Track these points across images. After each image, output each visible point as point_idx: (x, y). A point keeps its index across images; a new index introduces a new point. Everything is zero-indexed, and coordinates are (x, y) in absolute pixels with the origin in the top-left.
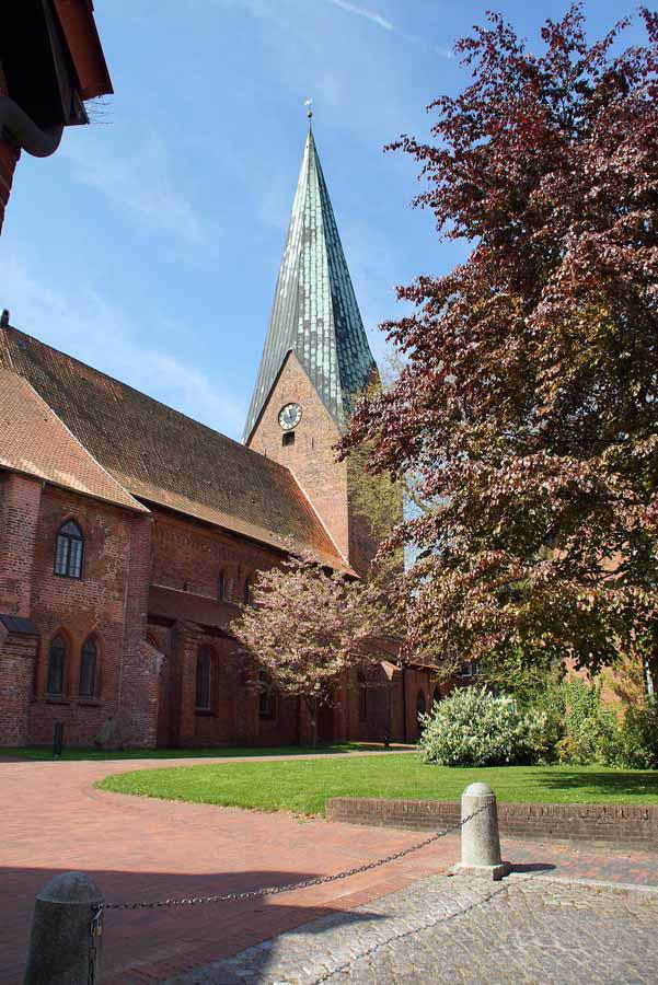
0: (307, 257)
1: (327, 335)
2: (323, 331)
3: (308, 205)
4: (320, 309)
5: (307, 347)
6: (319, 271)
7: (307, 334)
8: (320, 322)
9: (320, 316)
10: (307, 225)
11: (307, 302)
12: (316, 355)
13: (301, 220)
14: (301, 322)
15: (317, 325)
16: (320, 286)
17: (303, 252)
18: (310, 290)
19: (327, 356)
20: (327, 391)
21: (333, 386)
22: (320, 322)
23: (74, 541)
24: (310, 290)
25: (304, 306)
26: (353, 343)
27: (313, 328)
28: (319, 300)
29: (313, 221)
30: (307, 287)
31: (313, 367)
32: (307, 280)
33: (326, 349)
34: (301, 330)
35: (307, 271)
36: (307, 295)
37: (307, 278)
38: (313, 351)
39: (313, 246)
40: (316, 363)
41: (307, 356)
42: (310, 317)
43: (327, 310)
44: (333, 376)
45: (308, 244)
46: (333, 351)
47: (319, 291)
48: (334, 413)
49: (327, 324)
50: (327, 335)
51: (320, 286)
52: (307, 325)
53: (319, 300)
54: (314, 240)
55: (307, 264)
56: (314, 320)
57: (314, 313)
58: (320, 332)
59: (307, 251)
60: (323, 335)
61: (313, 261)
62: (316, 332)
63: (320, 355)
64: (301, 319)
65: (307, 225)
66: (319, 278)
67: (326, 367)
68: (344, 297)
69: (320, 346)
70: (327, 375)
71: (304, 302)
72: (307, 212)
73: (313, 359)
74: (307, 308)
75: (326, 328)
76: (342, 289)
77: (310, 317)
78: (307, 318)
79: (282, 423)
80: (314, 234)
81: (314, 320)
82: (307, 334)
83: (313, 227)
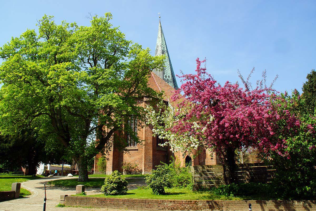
1: (171, 80)
4: (168, 73)
7: (166, 79)
13: (161, 47)
14: (164, 76)
27: (167, 78)
36: (165, 69)
47: (168, 68)
49: (171, 78)
50: (171, 80)
51: (168, 67)
52: (166, 77)
54: (165, 54)
57: (167, 74)
58: (169, 79)
60: (170, 80)
64: (164, 75)
69: (170, 83)
74: (165, 72)
75: (171, 78)
80: (165, 52)
81: (167, 76)
83: (164, 50)
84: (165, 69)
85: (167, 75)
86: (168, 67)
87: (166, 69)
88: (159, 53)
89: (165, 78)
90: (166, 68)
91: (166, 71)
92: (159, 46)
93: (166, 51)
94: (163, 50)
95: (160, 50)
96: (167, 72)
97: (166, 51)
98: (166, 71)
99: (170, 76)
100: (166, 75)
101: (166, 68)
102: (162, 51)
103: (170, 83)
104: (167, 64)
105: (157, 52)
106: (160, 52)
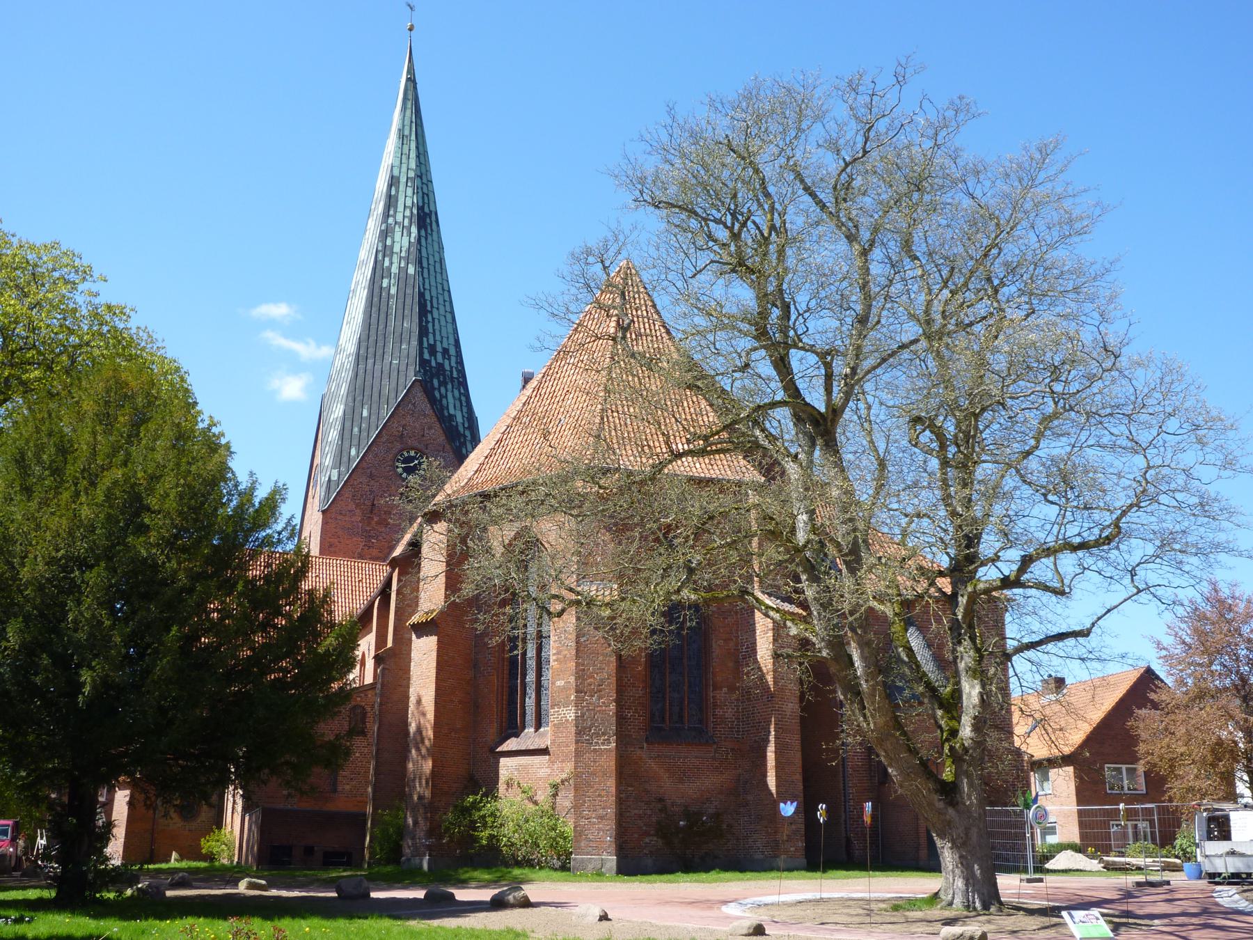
2: (451, 367)
4: (444, 334)
5: (436, 382)
7: (433, 364)
9: (445, 345)
12: (446, 397)
14: (425, 345)
15: (444, 358)
27: (439, 357)
28: (443, 323)
33: (456, 392)
36: (429, 308)
37: (427, 281)
39: (429, 237)
51: (441, 301)
53: (442, 319)
54: (429, 231)
58: (447, 367)
60: (451, 372)
61: (431, 262)
64: (425, 339)
69: (449, 386)
70: (461, 429)
71: (426, 318)
73: (444, 402)
74: (430, 325)
77: (435, 341)
80: (428, 221)
81: (439, 348)
84: (431, 312)
85: (438, 344)
86: (441, 301)
88: (399, 217)
89: (426, 356)
90: (432, 307)
92: (403, 180)
94: (423, 207)
96: (437, 327)
98: (433, 319)
100: (432, 342)
101: (432, 307)
102: (415, 211)
103: (449, 386)
104: (440, 287)
105: (391, 212)
106: (408, 213)
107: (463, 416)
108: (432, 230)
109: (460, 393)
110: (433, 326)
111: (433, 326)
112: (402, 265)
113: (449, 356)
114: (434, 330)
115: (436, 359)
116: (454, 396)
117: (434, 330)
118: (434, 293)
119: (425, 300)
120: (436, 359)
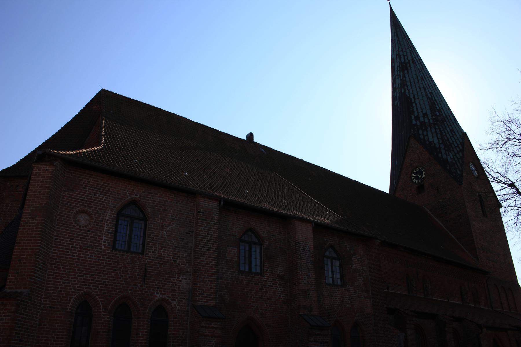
0: (408, 79)
1: (431, 122)
3: (400, 49)
5: (420, 132)
6: (417, 85)
7: (418, 124)
8: (425, 115)
9: (424, 111)
10: (403, 61)
11: (414, 105)
12: (427, 135)
13: (398, 59)
15: (424, 117)
16: (420, 94)
17: (404, 76)
18: (414, 98)
19: (435, 135)
20: (440, 155)
21: (443, 152)
22: (425, 115)
23: (333, 261)
24: (414, 98)
25: (413, 107)
26: (449, 124)
27: (422, 119)
28: (422, 102)
29: (406, 57)
30: (412, 96)
31: (428, 143)
32: (411, 92)
33: (433, 130)
34: (414, 122)
35: (409, 88)
36: (413, 101)
38: (425, 133)
39: (410, 72)
40: (428, 140)
41: (422, 137)
42: (418, 113)
43: (428, 107)
44: (442, 146)
45: (406, 72)
46: (438, 131)
47: (420, 98)
48: (448, 168)
50: (431, 122)
51: (420, 94)
52: (417, 118)
54: (409, 68)
55: (408, 84)
56: (421, 115)
57: (420, 110)
58: (426, 120)
59: (407, 75)
61: (412, 80)
62: (424, 122)
63: (430, 135)
64: (413, 116)
65: (403, 61)
66: (418, 89)
67: (436, 141)
68: (436, 98)
69: (429, 129)
70: (437, 146)
72: (401, 53)
73: (426, 138)
74: (415, 109)
75: (430, 117)
76: (434, 94)
77: (418, 113)
78: (416, 114)
79: (414, 180)
80: (408, 65)
81: (421, 115)
82: (418, 124)
83: (407, 61)
84: (415, 102)
87: (417, 101)
91: (416, 104)
93: (411, 62)
95: (398, 64)
96: (418, 106)
97: (411, 62)
98: (416, 104)
99: (429, 112)
101: (415, 99)
103: (429, 129)
107: (438, 139)
108: (411, 67)
109: (436, 129)
110: (417, 107)
111: (417, 107)
112: (400, 91)
113: (427, 116)
114: (417, 109)
115: (419, 121)
116: (432, 133)
117: (417, 109)
118: (415, 93)
119: (411, 99)
120: (419, 121)
